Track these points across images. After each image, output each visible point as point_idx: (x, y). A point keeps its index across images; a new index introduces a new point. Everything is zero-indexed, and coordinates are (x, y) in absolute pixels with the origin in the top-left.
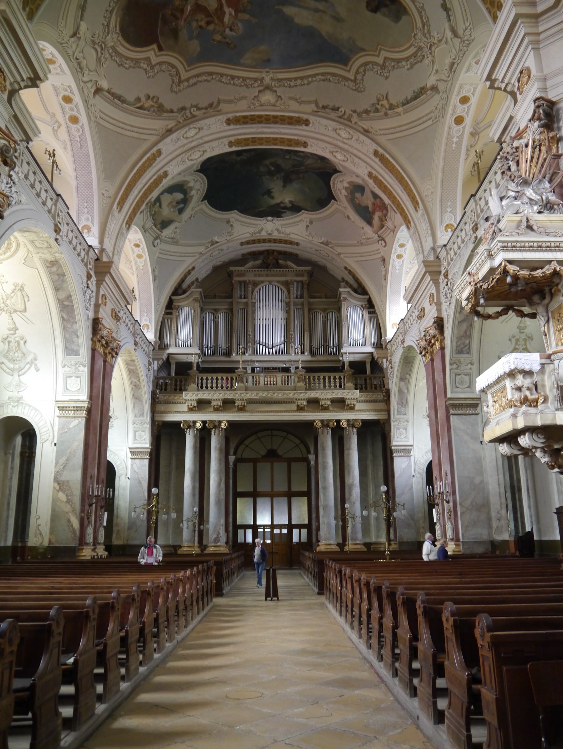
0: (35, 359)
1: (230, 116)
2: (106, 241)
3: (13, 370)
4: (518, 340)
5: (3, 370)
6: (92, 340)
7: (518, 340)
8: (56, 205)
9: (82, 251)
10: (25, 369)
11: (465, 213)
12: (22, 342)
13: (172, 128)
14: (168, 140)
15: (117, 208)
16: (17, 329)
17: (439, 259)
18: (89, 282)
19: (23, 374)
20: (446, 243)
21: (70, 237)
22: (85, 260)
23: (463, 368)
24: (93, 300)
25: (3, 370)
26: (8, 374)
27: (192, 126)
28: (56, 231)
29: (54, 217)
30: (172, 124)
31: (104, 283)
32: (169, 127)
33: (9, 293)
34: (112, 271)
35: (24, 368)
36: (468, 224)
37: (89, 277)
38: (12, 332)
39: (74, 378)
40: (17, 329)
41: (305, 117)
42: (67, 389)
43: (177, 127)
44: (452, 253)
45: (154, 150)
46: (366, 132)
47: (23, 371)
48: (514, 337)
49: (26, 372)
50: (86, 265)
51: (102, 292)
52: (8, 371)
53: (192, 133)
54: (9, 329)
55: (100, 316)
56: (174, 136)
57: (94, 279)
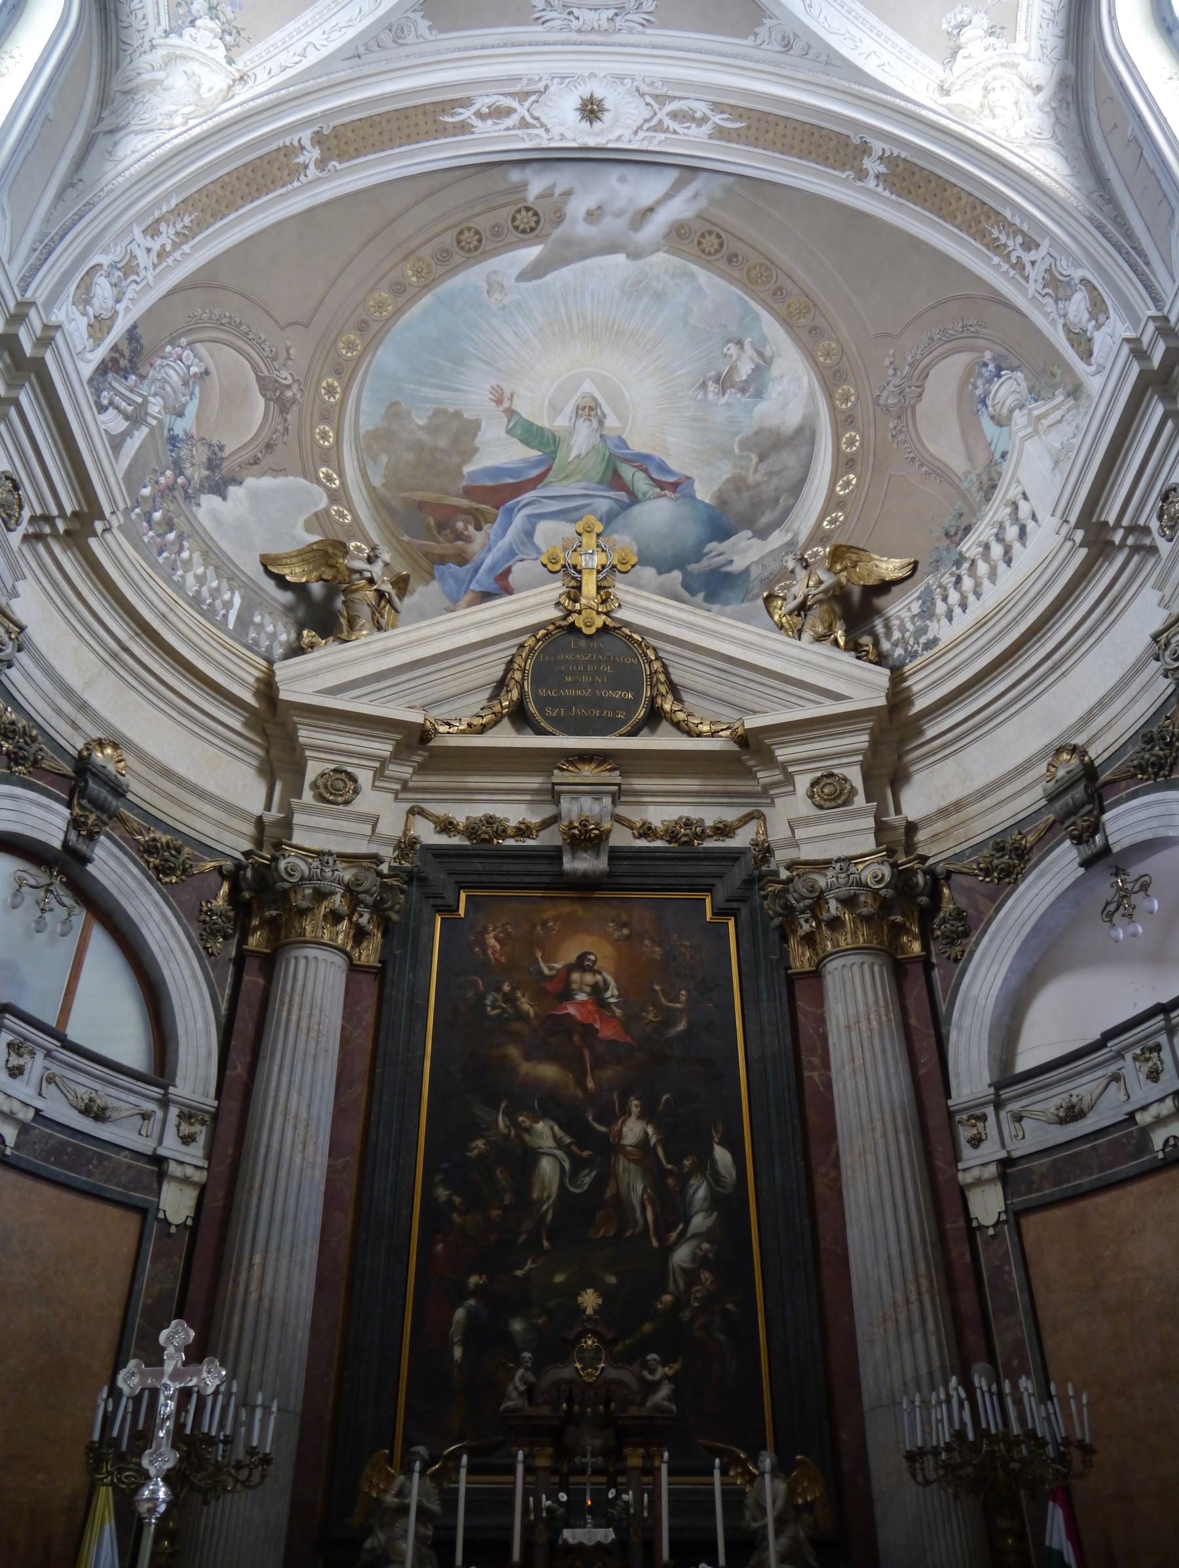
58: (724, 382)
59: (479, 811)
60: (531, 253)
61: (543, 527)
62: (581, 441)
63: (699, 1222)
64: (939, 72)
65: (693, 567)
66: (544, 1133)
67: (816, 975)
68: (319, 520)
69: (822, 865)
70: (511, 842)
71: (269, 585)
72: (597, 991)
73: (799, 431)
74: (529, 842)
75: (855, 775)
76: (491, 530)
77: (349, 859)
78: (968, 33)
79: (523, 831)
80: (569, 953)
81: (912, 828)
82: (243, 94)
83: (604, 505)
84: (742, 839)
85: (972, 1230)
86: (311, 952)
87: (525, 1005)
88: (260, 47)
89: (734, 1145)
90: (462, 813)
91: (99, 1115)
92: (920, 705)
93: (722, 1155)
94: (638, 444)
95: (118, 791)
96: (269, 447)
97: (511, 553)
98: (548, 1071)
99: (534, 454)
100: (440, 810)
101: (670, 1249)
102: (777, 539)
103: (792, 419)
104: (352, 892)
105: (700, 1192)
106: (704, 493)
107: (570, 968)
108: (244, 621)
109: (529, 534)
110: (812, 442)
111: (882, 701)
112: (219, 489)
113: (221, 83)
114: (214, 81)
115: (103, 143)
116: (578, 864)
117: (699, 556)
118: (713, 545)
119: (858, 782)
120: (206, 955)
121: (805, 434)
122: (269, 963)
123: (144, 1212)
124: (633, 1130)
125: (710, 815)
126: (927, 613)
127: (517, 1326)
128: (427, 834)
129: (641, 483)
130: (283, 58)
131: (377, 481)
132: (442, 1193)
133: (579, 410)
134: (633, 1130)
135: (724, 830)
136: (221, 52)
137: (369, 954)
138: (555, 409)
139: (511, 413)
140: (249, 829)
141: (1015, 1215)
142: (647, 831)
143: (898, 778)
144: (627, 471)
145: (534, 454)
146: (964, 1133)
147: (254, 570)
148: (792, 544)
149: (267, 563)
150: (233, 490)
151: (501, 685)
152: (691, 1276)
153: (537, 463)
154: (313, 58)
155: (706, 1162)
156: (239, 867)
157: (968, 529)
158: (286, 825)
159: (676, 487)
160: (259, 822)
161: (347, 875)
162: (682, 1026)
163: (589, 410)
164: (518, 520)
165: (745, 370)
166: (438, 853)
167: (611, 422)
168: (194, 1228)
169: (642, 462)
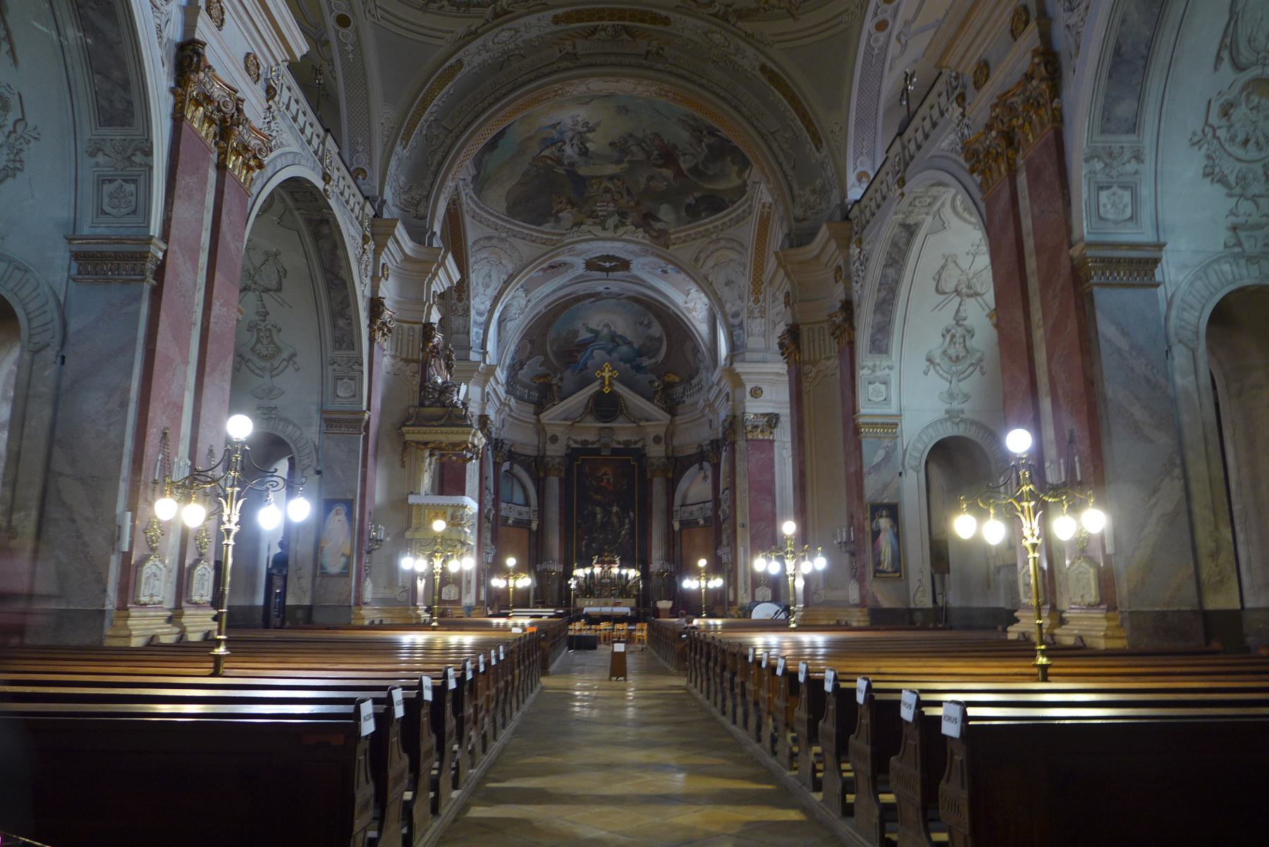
0: (294, 355)
1: (559, 11)
2: (387, 188)
3: (262, 369)
4: (953, 337)
5: (250, 369)
6: (370, 326)
7: (953, 337)
8: (324, 145)
9: (356, 204)
10: (281, 368)
11: (887, 158)
12: (274, 331)
13: (477, 28)
14: (472, 47)
15: (402, 143)
16: (268, 313)
17: (850, 220)
18: (365, 247)
19: (278, 375)
20: (858, 198)
21: (341, 186)
22: (360, 218)
23: (879, 373)
24: (370, 274)
25: (250, 369)
26: (257, 375)
27: (505, 26)
28: (324, 179)
29: (321, 160)
30: (477, 23)
31: (386, 249)
32: (473, 28)
33: (258, 266)
34: (396, 233)
35: (278, 367)
36: (890, 174)
37: (365, 240)
38: (262, 318)
39: (346, 380)
40: (268, 314)
41: (664, 13)
42: (338, 396)
43: (485, 28)
44: (868, 212)
45: (453, 60)
46: (748, 37)
47: (278, 370)
48: (948, 331)
49: (282, 372)
50: (361, 224)
51: (382, 261)
52: (257, 371)
53: (506, 34)
54: (257, 313)
55: (380, 295)
56: (479, 41)
57: (371, 243)
58: (641, 324)
59: (583, 438)
60: (593, 299)
61: (595, 352)
62: (605, 331)
63: (626, 527)
64: (685, 298)
65: (634, 363)
66: (598, 509)
67: (651, 480)
68: (542, 364)
69: (654, 458)
70: (590, 446)
71: (533, 384)
72: (608, 480)
73: (659, 338)
74: (594, 446)
75: (662, 435)
76: (582, 354)
77: (559, 457)
78: (691, 291)
79: (593, 443)
80: (603, 472)
81: (674, 448)
82: (530, 305)
83: (610, 346)
84: (639, 445)
85: (673, 531)
86: (553, 478)
87: (594, 483)
88: (533, 293)
89: (634, 511)
90: (579, 438)
91: (520, 514)
92: (678, 422)
93: (631, 514)
94: (619, 332)
95: (516, 453)
96: (531, 353)
97: (587, 359)
98: (599, 497)
99: (593, 335)
100: (575, 438)
101: (621, 532)
102: (653, 361)
103: (658, 335)
104: (559, 464)
105: (627, 521)
106: (636, 346)
107: (603, 474)
108: (529, 395)
109: (592, 353)
110: (662, 340)
111: (669, 422)
112: (522, 368)
113: (524, 302)
114: (523, 302)
115: (503, 324)
116: (605, 452)
117: (635, 360)
118: (637, 359)
119: (663, 438)
120: (533, 479)
121: (660, 339)
122: (544, 479)
123: (530, 529)
124: (615, 509)
125: (633, 438)
126: (684, 393)
127: (594, 545)
128: (574, 445)
129: (620, 341)
130: (539, 294)
131: (555, 349)
132: (579, 521)
133: (604, 326)
134: (615, 509)
135: (636, 443)
136: (524, 295)
137: (563, 474)
138: (598, 326)
139: (587, 327)
140: (536, 449)
141: (680, 530)
142: (619, 443)
143: (672, 435)
144: (617, 339)
145: (593, 335)
146: (675, 514)
147: (528, 381)
148: (657, 362)
149: (532, 379)
150: (525, 367)
151: (587, 405)
152: (625, 536)
153: (593, 337)
154: (544, 294)
155: (628, 516)
156: (536, 457)
157: (693, 378)
158: (545, 447)
159: (630, 343)
160: (538, 447)
161: (558, 460)
162: (625, 487)
163: (607, 325)
164: (589, 350)
165: (646, 322)
166: (574, 449)
167: (613, 328)
168: (537, 531)
169: (620, 337)
